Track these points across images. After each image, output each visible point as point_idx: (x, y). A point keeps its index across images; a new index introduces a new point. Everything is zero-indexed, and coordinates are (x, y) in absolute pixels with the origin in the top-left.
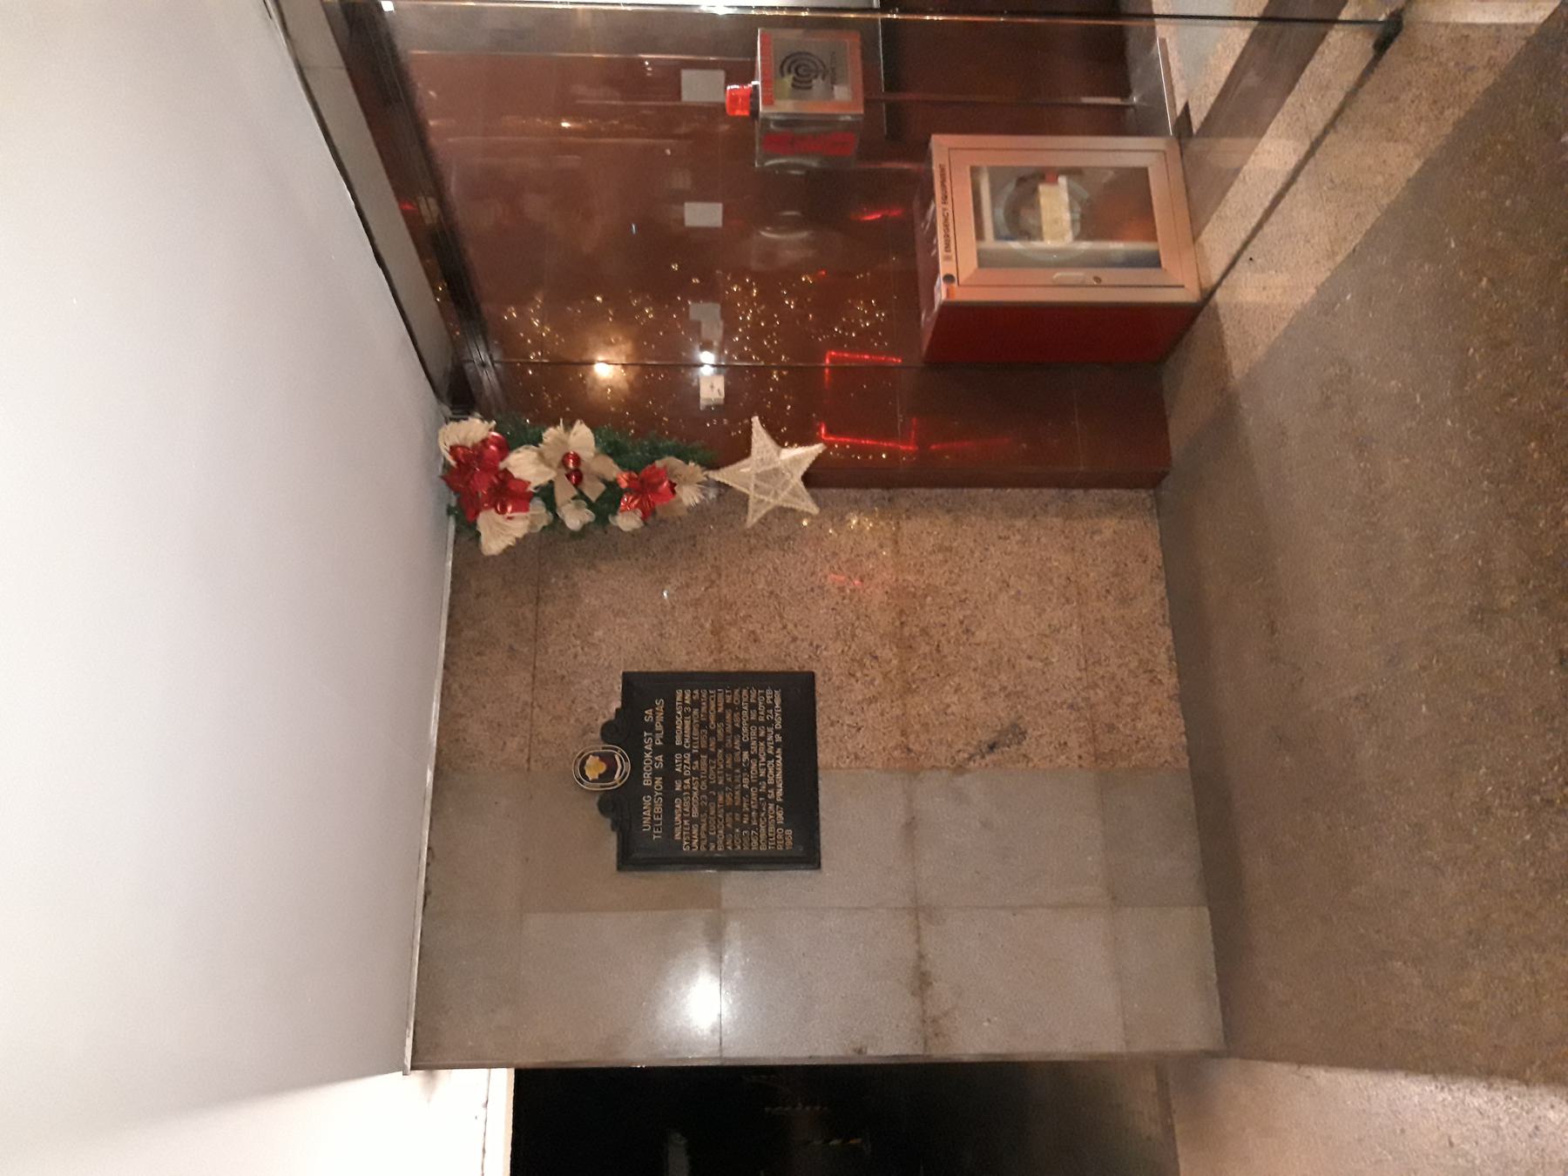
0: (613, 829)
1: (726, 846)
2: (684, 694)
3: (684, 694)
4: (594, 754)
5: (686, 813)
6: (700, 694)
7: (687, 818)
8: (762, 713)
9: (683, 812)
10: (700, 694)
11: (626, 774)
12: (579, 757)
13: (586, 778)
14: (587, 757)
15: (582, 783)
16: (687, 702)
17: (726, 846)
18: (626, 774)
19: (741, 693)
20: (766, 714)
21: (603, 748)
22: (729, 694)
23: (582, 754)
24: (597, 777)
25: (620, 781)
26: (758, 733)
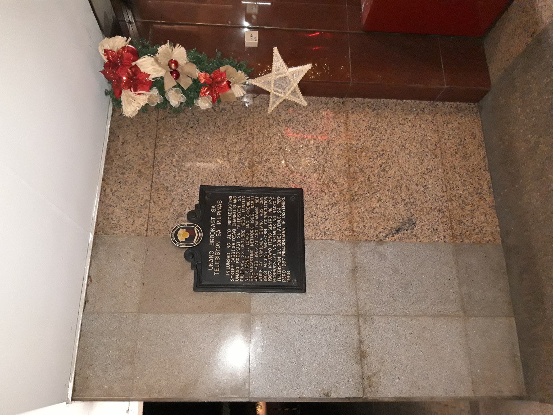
0: (192, 269)
1: (254, 279)
2: (233, 198)
3: (233, 198)
4: (183, 228)
5: (233, 261)
6: (242, 199)
7: (233, 264)
8: (275, 209)
9: (231, 260)
10: (242, 199)
11: (200, 238)
12: (175, 229)
13: (178, 241)
14: (179, 229)
15: (176, 243)
16: (235, 202)
17: (254, 279)
18: (200, 238)
19: (264, 198)
20: (277, 210)
21: (188, 225)
22: (257, 199)
23: (177, 227)
24: (184, 240)
25: (197, 243)
26: (272, 220)
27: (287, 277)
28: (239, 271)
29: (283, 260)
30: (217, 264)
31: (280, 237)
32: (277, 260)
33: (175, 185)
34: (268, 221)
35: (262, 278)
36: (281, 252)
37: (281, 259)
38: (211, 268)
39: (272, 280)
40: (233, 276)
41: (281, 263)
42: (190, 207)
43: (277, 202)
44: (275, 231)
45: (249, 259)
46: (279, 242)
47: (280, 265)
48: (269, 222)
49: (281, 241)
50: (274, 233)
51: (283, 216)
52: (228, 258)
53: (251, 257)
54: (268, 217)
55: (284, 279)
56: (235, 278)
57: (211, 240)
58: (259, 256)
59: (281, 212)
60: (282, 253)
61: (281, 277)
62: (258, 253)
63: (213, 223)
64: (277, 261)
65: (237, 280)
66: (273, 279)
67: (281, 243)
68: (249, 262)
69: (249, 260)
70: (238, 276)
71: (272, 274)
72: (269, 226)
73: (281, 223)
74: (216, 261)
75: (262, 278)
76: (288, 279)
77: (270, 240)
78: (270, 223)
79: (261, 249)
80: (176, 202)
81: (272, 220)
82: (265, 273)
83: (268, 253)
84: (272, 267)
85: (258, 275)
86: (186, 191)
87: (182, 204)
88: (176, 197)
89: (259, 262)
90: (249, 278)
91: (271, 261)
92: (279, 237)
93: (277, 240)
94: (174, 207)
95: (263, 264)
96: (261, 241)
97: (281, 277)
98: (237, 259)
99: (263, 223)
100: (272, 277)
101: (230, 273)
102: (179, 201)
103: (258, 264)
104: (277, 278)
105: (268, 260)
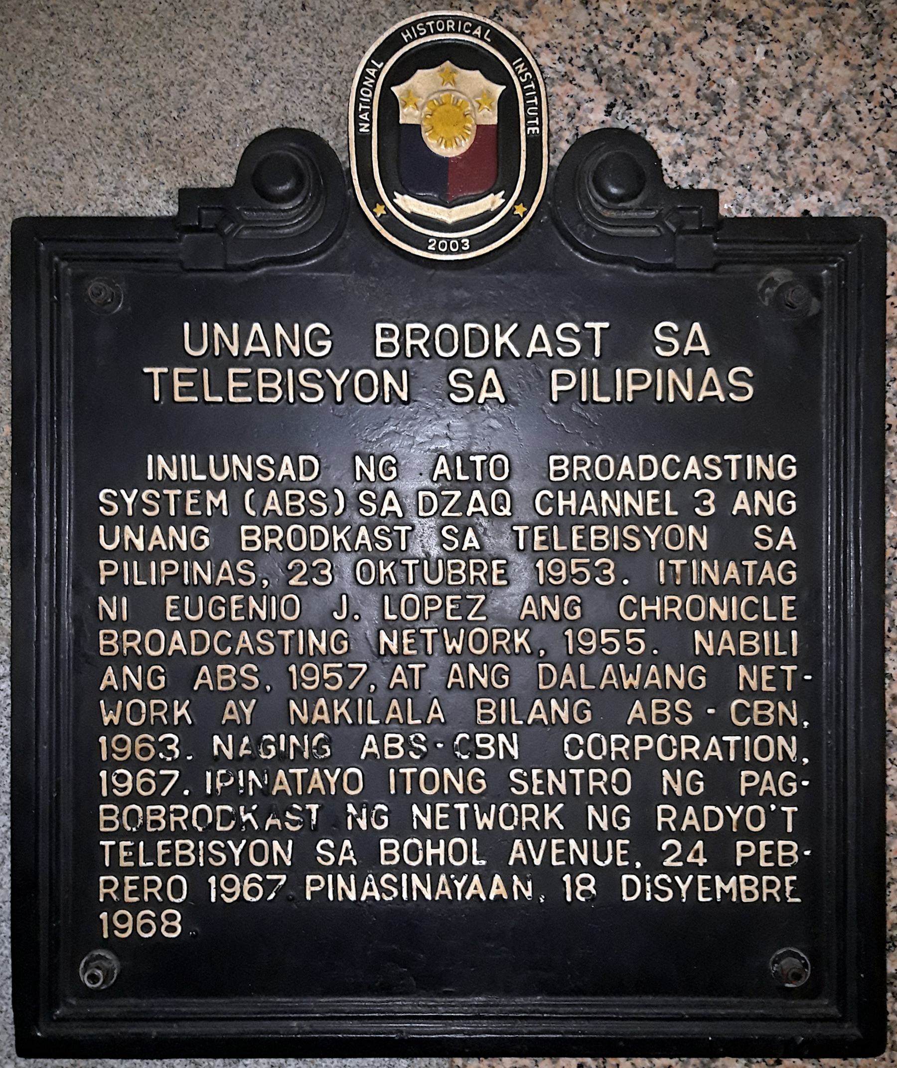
0: (186, 196)
1: (118, 661)
2: (775, 486)
3: (775, 486)
4: (507, 104)
5: (259, 502)
6: (775, 557)
7: (235, 501)
8: (690, 819)
9: (263, 490)
10: (775, 557)
11: (422, 242)
12: (498, 40)
13: (401, 73)
14: (495, 73)
15: (382, 54)
16: (741, 502)
17: (118, 661)
18: (422, 242)
20: (688, 837)
21: (535, 142)
22: (778, 677)
23: (513, 53)
24: (407, 116)
25: (389, 221)
26: (598, 799)
27: (135, 909)
28: (177, 554)
29: (268, 886)
30: (232, 385)
31: (458, 855)
32: (273, 834)
33: (877, 31)
34: (587, 763)
35: (123, 726)
36: (335, 869)
37: (281, 868)
38: (196, 343)
39: (111, 798)
40: (139, 504)
41: (245, 868)
42: (699, 162)
43: (756, 838)
44: (508, 820)
45: (277, 624)
46: (413, 847)
47: (230, 856)
48: (578, 772)
49: (421, 870)
50: (485, 810)
51: (631, 884)
52: (277, 467)
53: (294, 638)
54: (620, 761)
55: (120, 891)
56: (122, 519)
57: (417, 334)
58: (300, 695)
59: (671, 871)
60: (324, 871)
61: (136, 870)
62: (320, 691)
63: (555, 343)
64: (261, 833)
65: (110, 539)
66: (122, 802)
67: (410, 870)
68: (253, 624)
69: (264, 624)
70: (140, 544)
71: (155, 799)
72: (543, 777)
73: (578, 867)
74: (251, 378)
75: (123, 726)
76: (123, 919)
77: (430, 777)
78: (571, 778)
79: (352, 709)
80: (731, 51)
81: (598, 799)
82: (162, 746)
83: (323, 764)
84: (213, 799)
85: (146, 694)
86: (826, 118)
87: (716, 99)
88: (779, 49)
89: (247, 696)
90: (120, 625)
91: (265, 791)
92: (458, 848)
93: (435, 836)
94: (691, 38)
95: (237, 729)
96: (422, 712)
97: (136, 870)
98: (273, 534)
99: (573, 727)
100: (134, 797)
101: (168, 483)
102: (745, 71)
103: (239, 694)
104: (127, 835)
105: (267, 769)
